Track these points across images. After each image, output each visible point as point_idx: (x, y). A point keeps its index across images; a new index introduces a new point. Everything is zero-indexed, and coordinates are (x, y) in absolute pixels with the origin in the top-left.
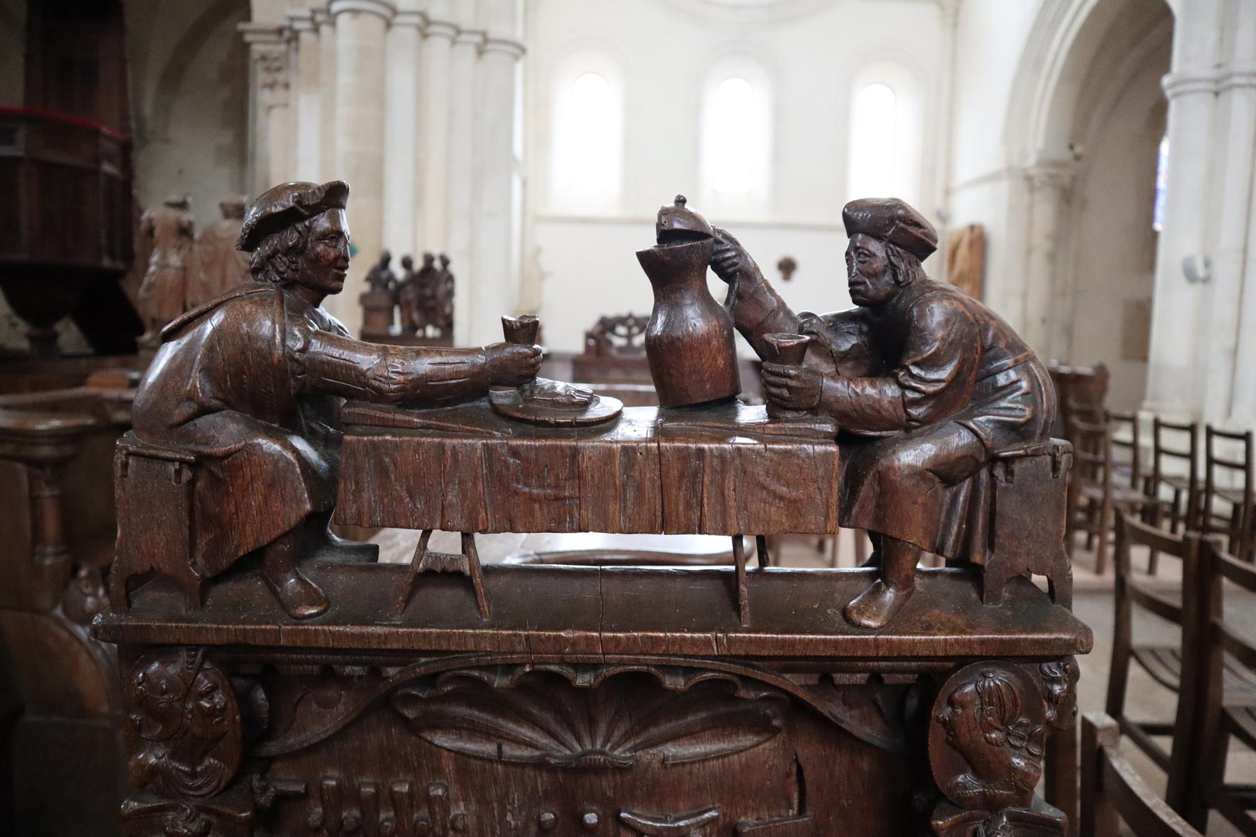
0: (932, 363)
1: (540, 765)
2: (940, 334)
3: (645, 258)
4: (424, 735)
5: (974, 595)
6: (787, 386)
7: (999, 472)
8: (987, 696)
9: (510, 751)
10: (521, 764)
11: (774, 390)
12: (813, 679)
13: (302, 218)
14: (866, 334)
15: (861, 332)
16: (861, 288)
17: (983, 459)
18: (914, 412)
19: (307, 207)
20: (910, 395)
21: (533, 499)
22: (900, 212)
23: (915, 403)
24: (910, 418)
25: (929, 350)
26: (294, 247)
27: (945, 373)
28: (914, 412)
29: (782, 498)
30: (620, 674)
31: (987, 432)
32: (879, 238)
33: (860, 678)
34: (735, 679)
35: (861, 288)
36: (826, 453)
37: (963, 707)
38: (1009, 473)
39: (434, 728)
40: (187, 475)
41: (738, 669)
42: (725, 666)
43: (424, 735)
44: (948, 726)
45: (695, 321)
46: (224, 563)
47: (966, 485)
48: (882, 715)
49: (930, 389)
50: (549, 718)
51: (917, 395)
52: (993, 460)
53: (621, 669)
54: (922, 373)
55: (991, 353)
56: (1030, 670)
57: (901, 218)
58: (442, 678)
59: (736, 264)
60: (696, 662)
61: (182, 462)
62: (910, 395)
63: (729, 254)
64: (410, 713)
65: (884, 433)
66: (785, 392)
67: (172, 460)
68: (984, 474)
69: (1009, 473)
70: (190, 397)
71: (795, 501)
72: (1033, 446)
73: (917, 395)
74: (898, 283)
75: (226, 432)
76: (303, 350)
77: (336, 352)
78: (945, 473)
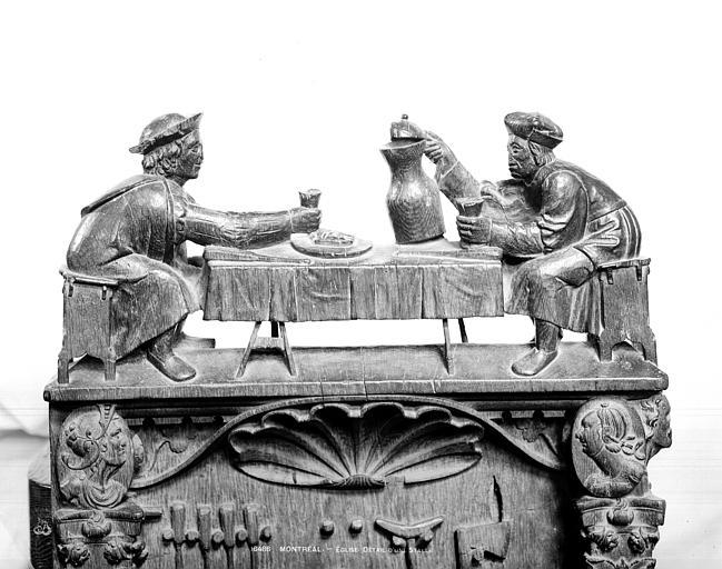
0: (556, 212)
1: (325, 487)
2: (561, 195)
3: (386, 153)
4: (245, 469)
5: (596, 357)
6: (471, 230)
7: (604, 278)
8: (603, 419)
9: (302, 479)
10: (311, 487)
11: (462, 232)
12: (498, 415)
13: (181, 136)
14: (524, 194)
15: (519, 192)
16: (515, 167)
17: (591, 270)
18: (548, 242)
19: (184, 131)
20: (545, 232)
21: (322, 299)
22: (536, 123)
23: (548, 237)
24: (546, 247)
25: (554, 205)
26: (175, 154)
27: (566, 218)
28: (548, 242)
29: (469, 295)
30: (379, 406)
31: (594, 254)
32: (525, 138)
33: (529, 414)
34: (448, 411)
35: (515, 167)
36: (494, 269)
37: (590, 426)
38: (609, 277)
39: (251, 462)
40: (109, 294)
41: (449, 402)
42: (440, 401)
43: (245, 469)
44: (583, 440)
45: (413, 190)
46: (131, 348)
47: (586, 287)
48: (550, 447)
49: (556, 228)
50: (327, 455)
51: (550, 233)
52: (600, 270)
53: (377, 404)
54: (552, 219)
55: (595, 205)
56: (635, 404)
57: (535, 127)
58: (264, 417)
59: (439, 154)
60: (422, 399)
61: (108, 286)
62: (545, 232)
63: (437, 147)
64: (238, 449)
65: (532, 256)
66: (469, 232)
67: (101, 285)
68: (596, 281)
69: (609, 277)
70: (115, 245)
71: (478, 297)
72: (624, 259)
73: (550, 233)
74: (537, 164)
75: (136, 266)
76: (184, 215)
77: (203, 217)
78: (572, 279)
